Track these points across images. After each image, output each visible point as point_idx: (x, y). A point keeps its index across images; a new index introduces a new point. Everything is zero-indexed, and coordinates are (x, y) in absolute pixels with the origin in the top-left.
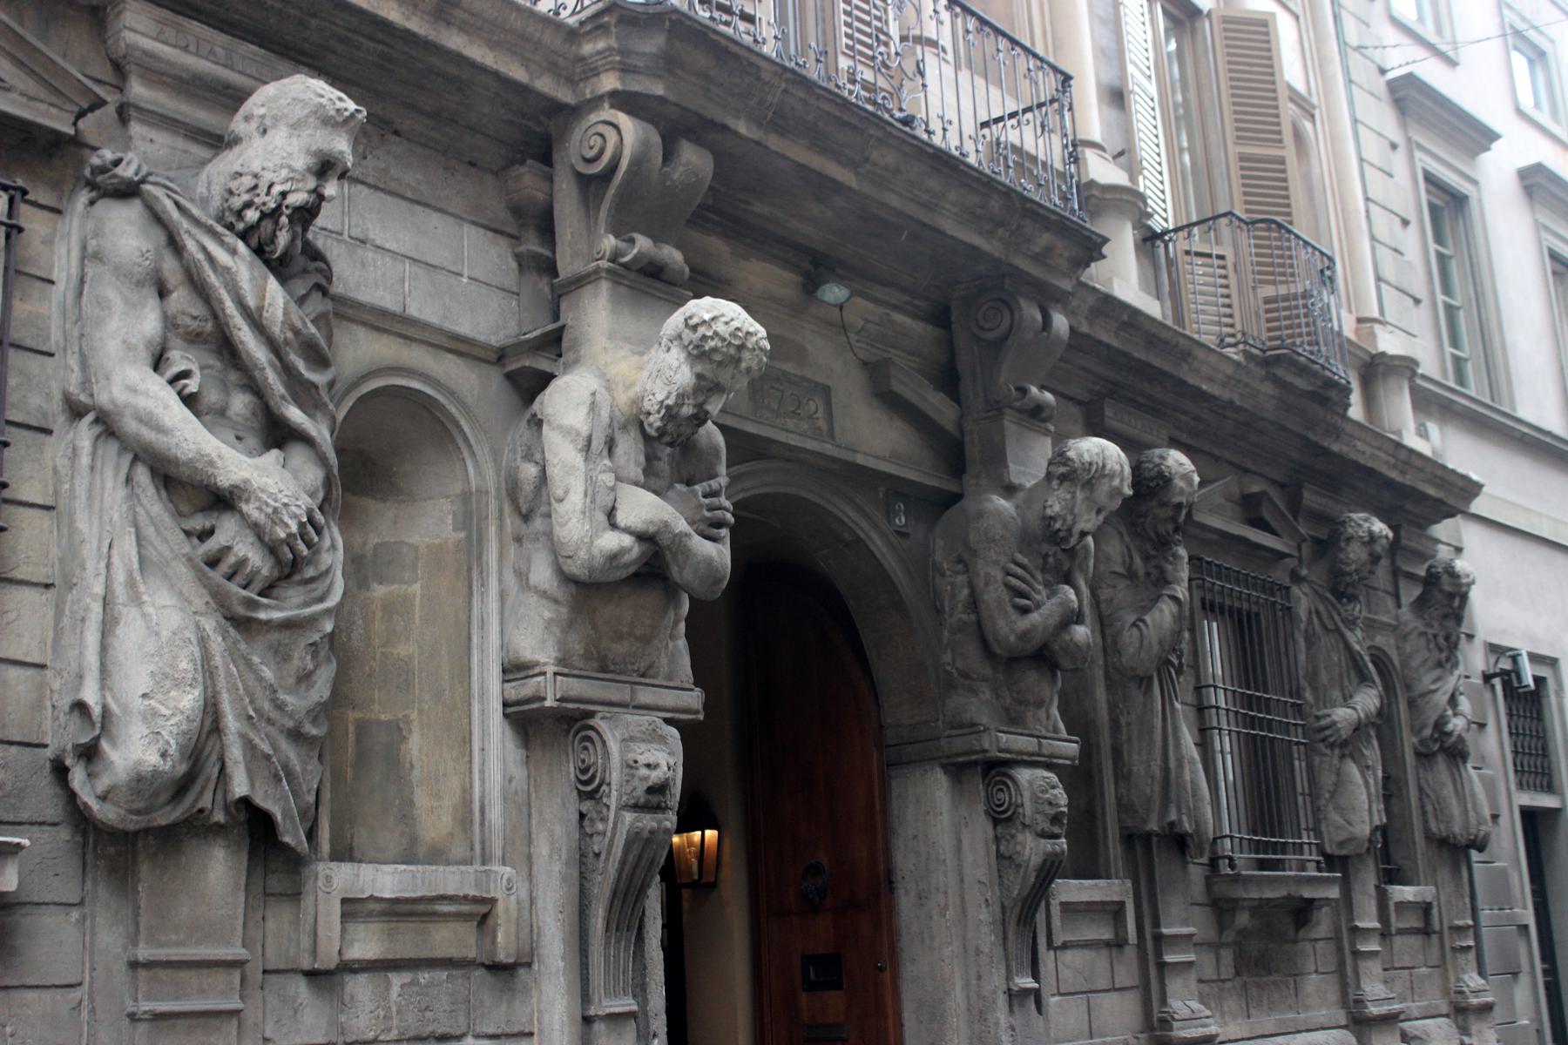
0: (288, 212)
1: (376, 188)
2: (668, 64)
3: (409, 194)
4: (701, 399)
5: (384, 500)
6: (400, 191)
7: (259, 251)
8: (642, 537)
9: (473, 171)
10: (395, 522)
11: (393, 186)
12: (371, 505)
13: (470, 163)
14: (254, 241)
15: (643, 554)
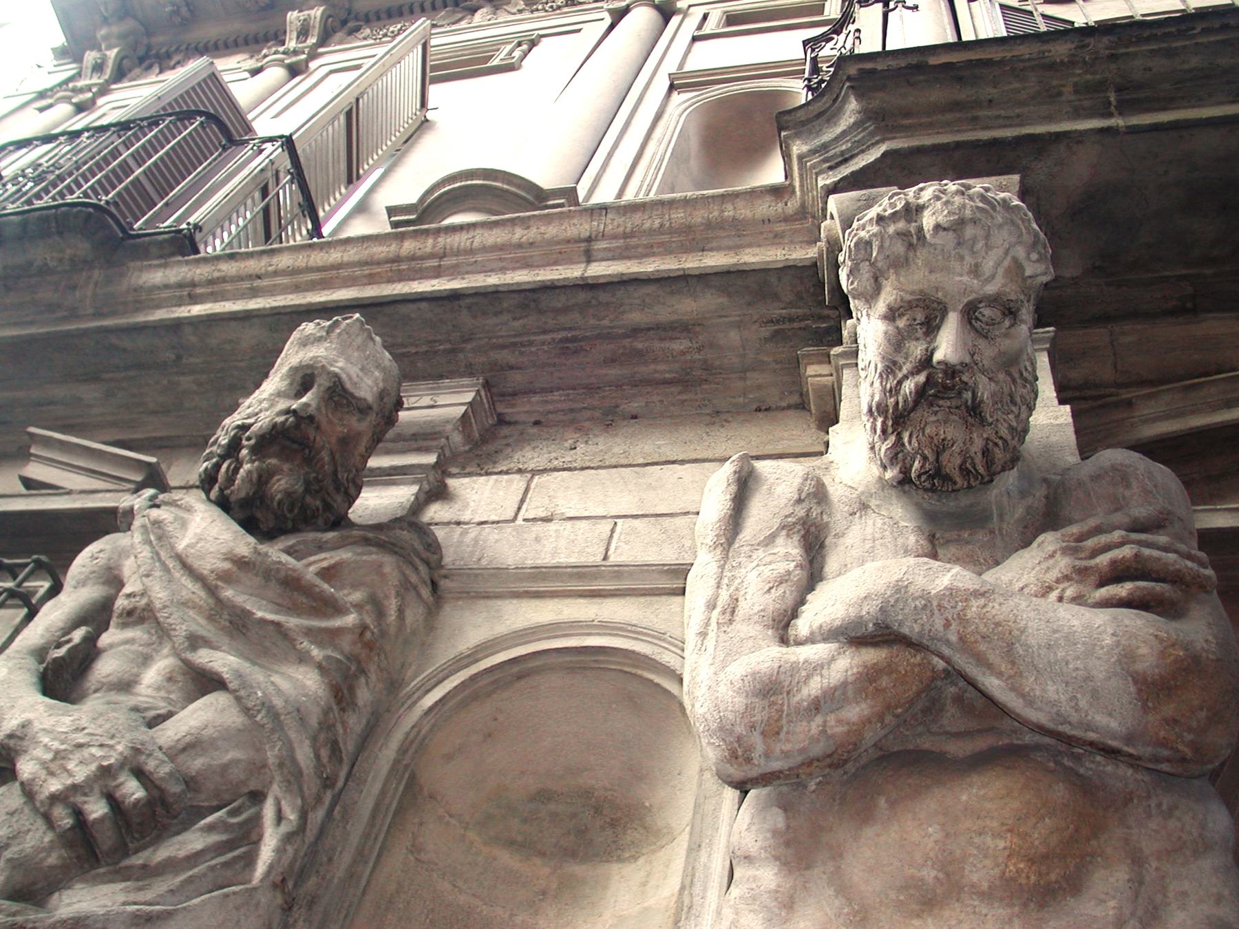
0: (252, 442)
1: (583, 469)
2: (879, 121)
3: (641, 461)
4: (917, 350)
5: (635, 858)
6: (625, 462)
7: (224, 504)
8: (854, 635)
9: (760, 415)
10: (644, 884)
11: (613, 461)
12: (615, 867)
13: (759, 410)
14: (214, 493)
15: (868, 679)
